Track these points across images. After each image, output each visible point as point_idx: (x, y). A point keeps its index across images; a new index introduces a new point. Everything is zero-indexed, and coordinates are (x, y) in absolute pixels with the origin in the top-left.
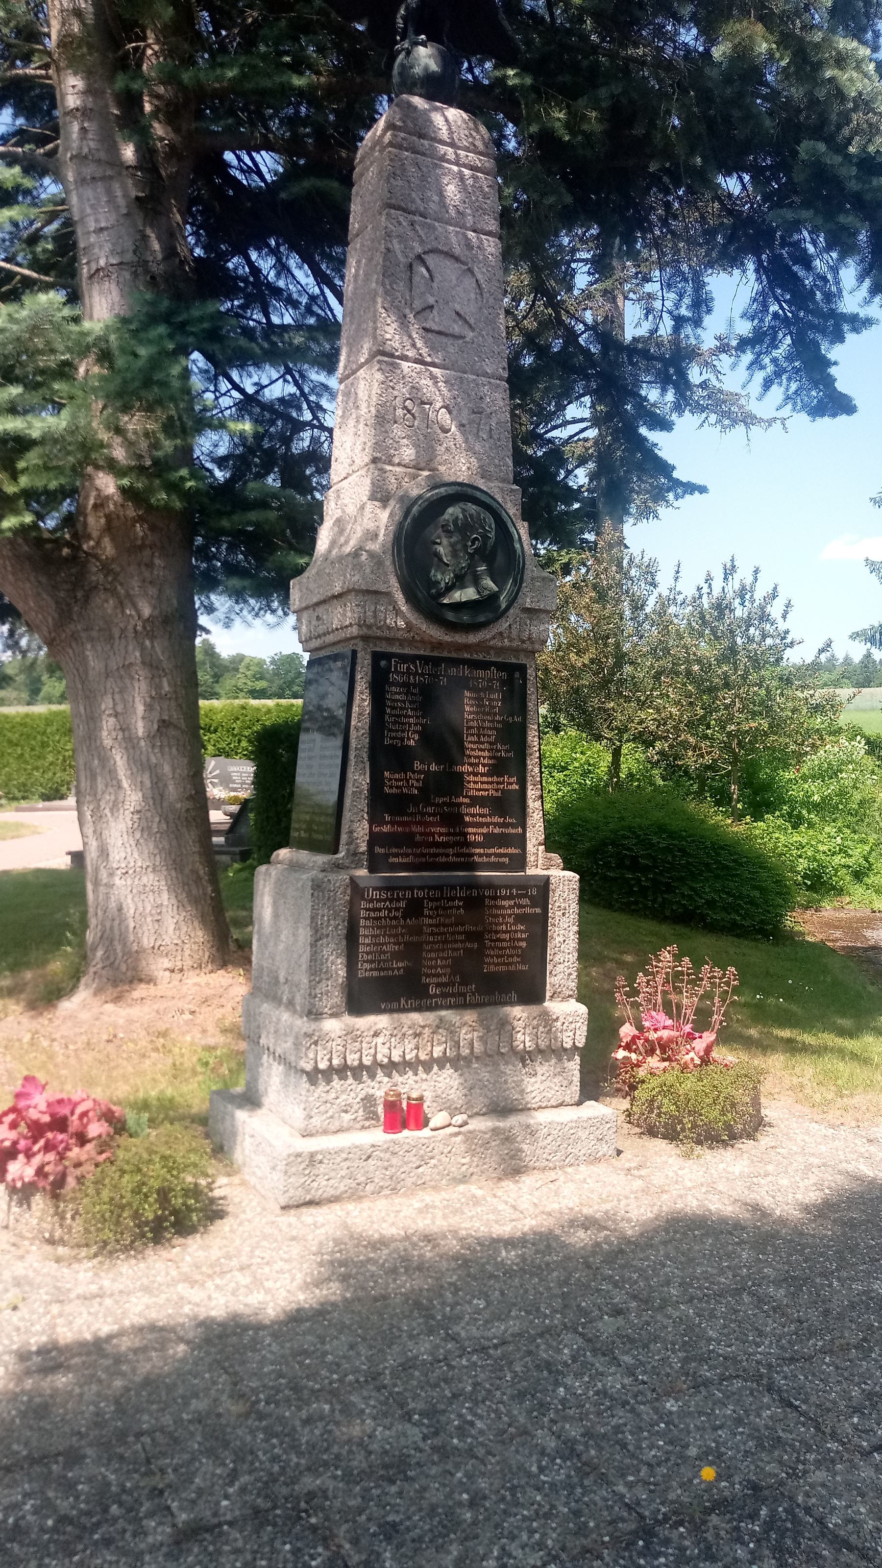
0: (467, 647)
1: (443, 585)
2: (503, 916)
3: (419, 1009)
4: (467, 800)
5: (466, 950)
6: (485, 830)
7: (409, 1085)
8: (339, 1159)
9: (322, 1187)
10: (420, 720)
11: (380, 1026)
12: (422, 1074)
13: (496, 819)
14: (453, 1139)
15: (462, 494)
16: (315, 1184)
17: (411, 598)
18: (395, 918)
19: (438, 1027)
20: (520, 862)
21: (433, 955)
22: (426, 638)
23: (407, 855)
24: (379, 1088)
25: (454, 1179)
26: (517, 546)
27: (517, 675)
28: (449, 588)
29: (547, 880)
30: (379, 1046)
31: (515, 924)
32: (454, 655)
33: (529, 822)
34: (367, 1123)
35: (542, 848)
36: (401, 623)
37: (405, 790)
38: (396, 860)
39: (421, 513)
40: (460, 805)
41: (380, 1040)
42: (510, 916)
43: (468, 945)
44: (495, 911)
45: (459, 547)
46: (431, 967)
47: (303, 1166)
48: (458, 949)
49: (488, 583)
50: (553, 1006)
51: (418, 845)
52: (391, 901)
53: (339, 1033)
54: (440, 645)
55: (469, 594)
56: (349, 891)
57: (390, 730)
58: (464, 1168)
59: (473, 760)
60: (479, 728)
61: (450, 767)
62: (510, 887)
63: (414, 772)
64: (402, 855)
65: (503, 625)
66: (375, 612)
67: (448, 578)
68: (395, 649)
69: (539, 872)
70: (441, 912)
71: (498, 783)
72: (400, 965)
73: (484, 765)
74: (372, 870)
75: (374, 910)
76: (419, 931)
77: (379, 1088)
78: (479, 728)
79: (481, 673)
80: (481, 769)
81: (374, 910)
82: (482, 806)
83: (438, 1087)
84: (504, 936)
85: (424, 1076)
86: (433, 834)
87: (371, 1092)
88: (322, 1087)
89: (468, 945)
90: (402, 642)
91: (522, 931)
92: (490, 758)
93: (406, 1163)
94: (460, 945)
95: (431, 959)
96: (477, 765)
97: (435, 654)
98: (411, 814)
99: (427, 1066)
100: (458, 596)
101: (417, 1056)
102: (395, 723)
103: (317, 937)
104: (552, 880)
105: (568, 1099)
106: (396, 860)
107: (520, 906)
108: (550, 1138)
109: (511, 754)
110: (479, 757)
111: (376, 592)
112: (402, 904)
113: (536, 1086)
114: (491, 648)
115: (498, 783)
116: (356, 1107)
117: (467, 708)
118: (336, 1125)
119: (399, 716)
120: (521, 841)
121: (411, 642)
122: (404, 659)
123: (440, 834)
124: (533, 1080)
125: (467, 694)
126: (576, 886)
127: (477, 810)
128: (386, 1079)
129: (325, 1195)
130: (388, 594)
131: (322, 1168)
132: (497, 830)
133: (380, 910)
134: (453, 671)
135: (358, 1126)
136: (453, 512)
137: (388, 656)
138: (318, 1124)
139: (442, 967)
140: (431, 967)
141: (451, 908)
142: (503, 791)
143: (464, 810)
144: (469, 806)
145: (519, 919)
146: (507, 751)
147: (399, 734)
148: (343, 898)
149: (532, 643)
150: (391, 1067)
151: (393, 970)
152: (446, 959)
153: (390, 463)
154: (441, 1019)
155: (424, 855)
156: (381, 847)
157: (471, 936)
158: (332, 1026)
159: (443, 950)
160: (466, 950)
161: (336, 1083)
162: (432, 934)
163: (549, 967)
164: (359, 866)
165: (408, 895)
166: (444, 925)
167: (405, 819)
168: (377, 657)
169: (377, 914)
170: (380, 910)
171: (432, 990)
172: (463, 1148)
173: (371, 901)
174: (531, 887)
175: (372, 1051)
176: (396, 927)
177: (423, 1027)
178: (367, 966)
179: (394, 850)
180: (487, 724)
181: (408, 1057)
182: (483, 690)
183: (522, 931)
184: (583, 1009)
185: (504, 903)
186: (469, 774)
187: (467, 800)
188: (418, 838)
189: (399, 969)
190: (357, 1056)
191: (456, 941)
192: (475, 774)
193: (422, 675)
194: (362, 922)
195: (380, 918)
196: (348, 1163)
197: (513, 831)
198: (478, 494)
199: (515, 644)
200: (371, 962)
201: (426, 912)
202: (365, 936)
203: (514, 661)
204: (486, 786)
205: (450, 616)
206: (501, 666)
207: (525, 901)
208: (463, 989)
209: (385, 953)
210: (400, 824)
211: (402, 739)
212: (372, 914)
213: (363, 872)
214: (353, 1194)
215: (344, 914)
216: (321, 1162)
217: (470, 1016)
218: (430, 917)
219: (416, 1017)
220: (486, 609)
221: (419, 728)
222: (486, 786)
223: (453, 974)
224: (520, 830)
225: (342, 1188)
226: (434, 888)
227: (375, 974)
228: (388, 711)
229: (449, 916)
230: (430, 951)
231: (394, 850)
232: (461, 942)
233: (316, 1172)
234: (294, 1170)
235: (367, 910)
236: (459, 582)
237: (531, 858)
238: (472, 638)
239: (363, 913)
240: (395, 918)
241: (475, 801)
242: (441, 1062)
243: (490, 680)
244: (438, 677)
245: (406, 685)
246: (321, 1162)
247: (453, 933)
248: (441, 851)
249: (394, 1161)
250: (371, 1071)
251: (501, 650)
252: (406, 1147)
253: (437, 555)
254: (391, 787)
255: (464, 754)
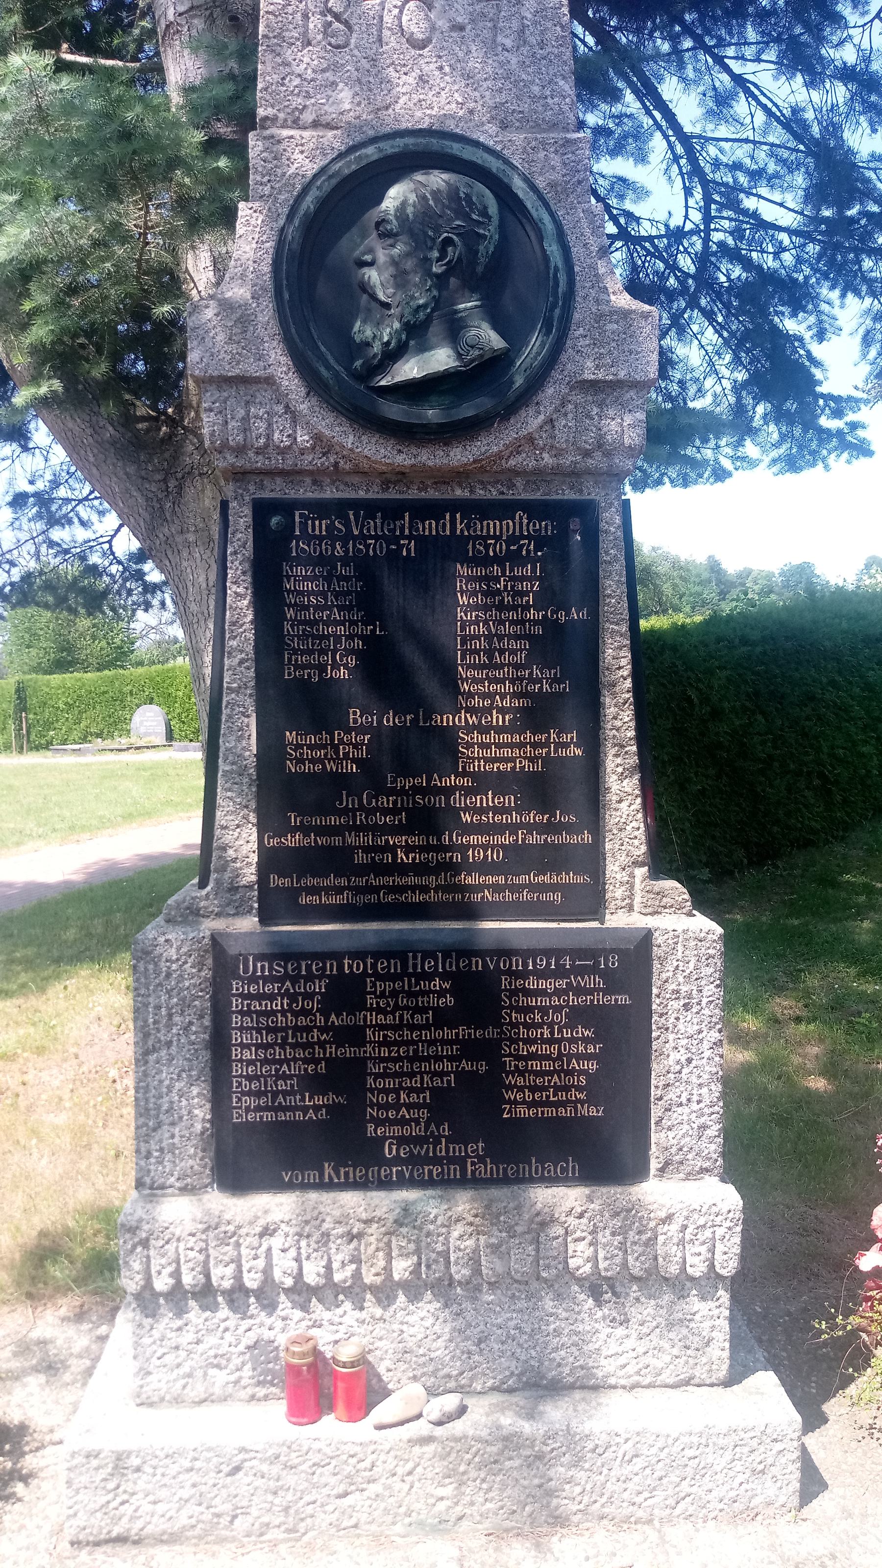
0: (460, 475)
1: (377, 348)
2: (544, 1011)
3: (362, 1185)
4: (466, 782)
5: (460, 1075)
6: (507, 839)
7: (342, 1333)
8: (174, 1469)
9: (145, 1512)
10: (359, 629)
11: (276, 1216)
12: (372, 1309)
13: (532, 817)
14: (417, 1450)
15: (422, 151)
16: (128, 1509)
17: (314, 383)
18: (305, 1012)
19: (399, 1223)
20: (593, 901)
21: (390, 1083)
22: (365, 465)
23: (339, 890)
24: (286, 1328)
25: (421, 1524)
26: (553, 249)
27: (575, 524)
28: (394, 354)
29: (647, 936)
30: (275, 1252)
31: (571, 1025)
32: (432, 494)
33: (612, 819)
34: (261, 1392)
35: (641, 872)
36: (303, 438)
37: (330, 766)
38: (315, 900)
39: (324, 204)
40: (448, 791)
41: (276, 1242)
42: (558, 1009)
43: (466, 1065)
44: (523, 1001)
45: (409, 264)
46: (387, 1107)
47: (103, 1474)
48: (441, 1074)
49: (491, 338)
50: (655, 1192)
51: (362, 870)
52: (294, 980)
53: (190, 1227)
54: (401, 476)
55: (441, 359)
56: (209, 962)
57: (295, 652)
58: (442, 1506)
59: (476, 702)
60: (489, 637)
61: (428, 717)
62: (558, 953)
63: (348, 731)
64: (327, 890)
65: (531, 421)
66: (246, 419)
67: (388, 331)
68: (305, 492)
69: (638, 921)
70: (403, 1001)
71: (535, 745)
72: (319, 1101)
73: (502, 711)
74: (265, 918)
75: (260, 997)
76: (354, 1035)
77: (286, 1328)
78: (489, 637)
79: (493, 526)
80: (497, 719)
81: (260, 997)
82: (499, 792)
83: (401, 1337)
84: (545, 1049)
85: (378, 1312)
86: (393, 850)
87: (267, 1335)
88: (167, 1321)
89: (466, 1065)
90: (316, 477)
91: (586, 1040)
92: (515, 695)
93: (315, 1486)
94: (447, 1066)
95: (386, 1091)
96: (488, 711)
97: (392, 494)
98: (345, 811)
99: (385, 1293)
100: (410, 369)
101: (357, 1275)
102: (305, 636)
103: (146, 1049)
104: (658, 939)
105: (700, 1373)
106: (315, 900)
107: (579, 991)
108: (639, 1463)
109: (566, 686)
110: (491, 696)
111: (243, 380)
112: (319, 987)
113: (629, 1344)
114: (515, 472)
115: (535, 745)
116: (237, 1361)
117: (463, 600)
118: (198, 1390)
119: (314, 623)
120: (593, 860)
121: (336, 474)
122: (321, 509)
123: (408, 849)
124: (620, 1331)
125: (463, 570)
126: (716, 949)
127: (489, 799)
128: (298, 1314)
129: (149, 1529)
130: (269, 381)
131: (143, 1482)
132: (535, 839)
133: (271, 997)
134: (429, 527)
135: (244, 1394)
136: (396, 196)
137: (286, 507)
138: (164, 1387)
139: (409, 1106)
140: (387, 1107)
141: (427, 993)
142: (547, 760)
143: (458, 800)
144: (469, 792)
145: (577, 1016)
146: (555, 680)
147: (314, 659)
148: (193, 977)
149: (608, 454)
150: (303, 1293)
151: (305, 1110)
152: (419, 1091)
153: (296, 124)
154: (406, 1209)
155: (375, 890)
156: (281, 875)
157: (469, 1049)
158: (178, 1212)
159: (412, 1075)
160: (460, 1075)
161: (195, 1314)
162: (385, 1043)
163: (656, 1112)
164: (240, 911)
165: (331, 967)
166: (412, 1027)
167: (333, 820)
168: (262, 510)
169: (266, 1005)
170: (271, 997)
171: (389, 1151)
172: (439, 1467)
173: (253, 980)
174: (606, 952)
175: (261, 1263)
176: (308, 1029)
177: (368, 1222)
178: (247, 1101)
179: (311, 881)
180: (508, 629)
181: (337, 1277)
182: (499, 560)
183: (586, 1040)
184: (729, 1198)
185: (543, 984)
186: (469, 729)
187: (466, 782)
188: (360, 858)
189: (317, 1108)
190: (230, 1270)
191: (438, 1058)
192: (483, 730)
193: (363, 538)
194: (236, 1020)
195: (273, 1013)
196: (194, 1477)
197: (575, 839)
198: (456, 148)
199: (567, 461)
200: (258, 1094)
201: (371, 1000)
202: (243, 1046)
203: (570, 495)
204: (507, 752)
205: (393, 410)
206: (537, 510)
207: (588, 981)
208: (457, 1150)
209: (285, 1077)
210: (322, 831)
211: (322, 668)
212: (256, 1006)
213: (249, 923)
214: (206, 1533)
215: (203, 1003)
216: (138, 1470)
217: (464, 1203)
218: (379, 1010)
219: (352, 1201)
220: (484, 390)
221: (359, 644)
222: (507, 752)
223: (435, 1118)
224: (587, 838)
225: (183, 1520)
226: (388, 954)
227: (268, 1116)
228: (290, 613)
229: (423, 1010)
230: (384, 1075)
231: (311, 881)
232: (451, 1059)
233: (130, 1487)
234: (84, 1479)
235: (243, 996)
236: (415, 336)
237: (615, 893)
238: (459, 455)
239: (236, 1003)
240: (305, 1012)
241: (481, 783)
242: (414, 1289)
243: (513, 539)
244: (396, 540)
245: (322, 560)
246: (138, 1470)
247: (432, 1043)
248: (412, 880)
249: (290, 1479)
250: (266, 1295)
251: (538, 476)
252: (315, 1458)
253: (365, 288)
254: (300, 761)
255: (457, 691)
